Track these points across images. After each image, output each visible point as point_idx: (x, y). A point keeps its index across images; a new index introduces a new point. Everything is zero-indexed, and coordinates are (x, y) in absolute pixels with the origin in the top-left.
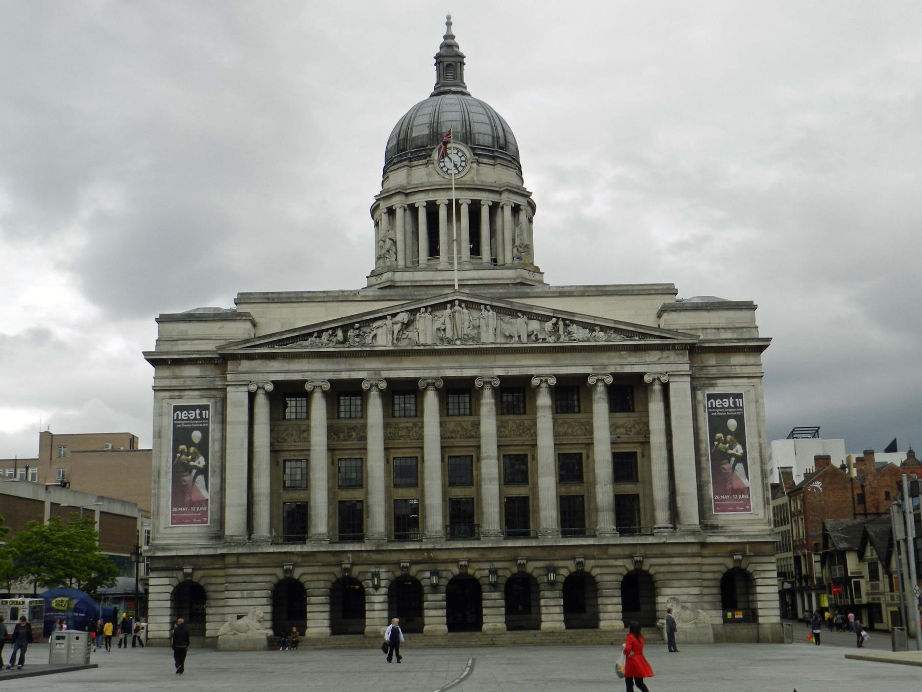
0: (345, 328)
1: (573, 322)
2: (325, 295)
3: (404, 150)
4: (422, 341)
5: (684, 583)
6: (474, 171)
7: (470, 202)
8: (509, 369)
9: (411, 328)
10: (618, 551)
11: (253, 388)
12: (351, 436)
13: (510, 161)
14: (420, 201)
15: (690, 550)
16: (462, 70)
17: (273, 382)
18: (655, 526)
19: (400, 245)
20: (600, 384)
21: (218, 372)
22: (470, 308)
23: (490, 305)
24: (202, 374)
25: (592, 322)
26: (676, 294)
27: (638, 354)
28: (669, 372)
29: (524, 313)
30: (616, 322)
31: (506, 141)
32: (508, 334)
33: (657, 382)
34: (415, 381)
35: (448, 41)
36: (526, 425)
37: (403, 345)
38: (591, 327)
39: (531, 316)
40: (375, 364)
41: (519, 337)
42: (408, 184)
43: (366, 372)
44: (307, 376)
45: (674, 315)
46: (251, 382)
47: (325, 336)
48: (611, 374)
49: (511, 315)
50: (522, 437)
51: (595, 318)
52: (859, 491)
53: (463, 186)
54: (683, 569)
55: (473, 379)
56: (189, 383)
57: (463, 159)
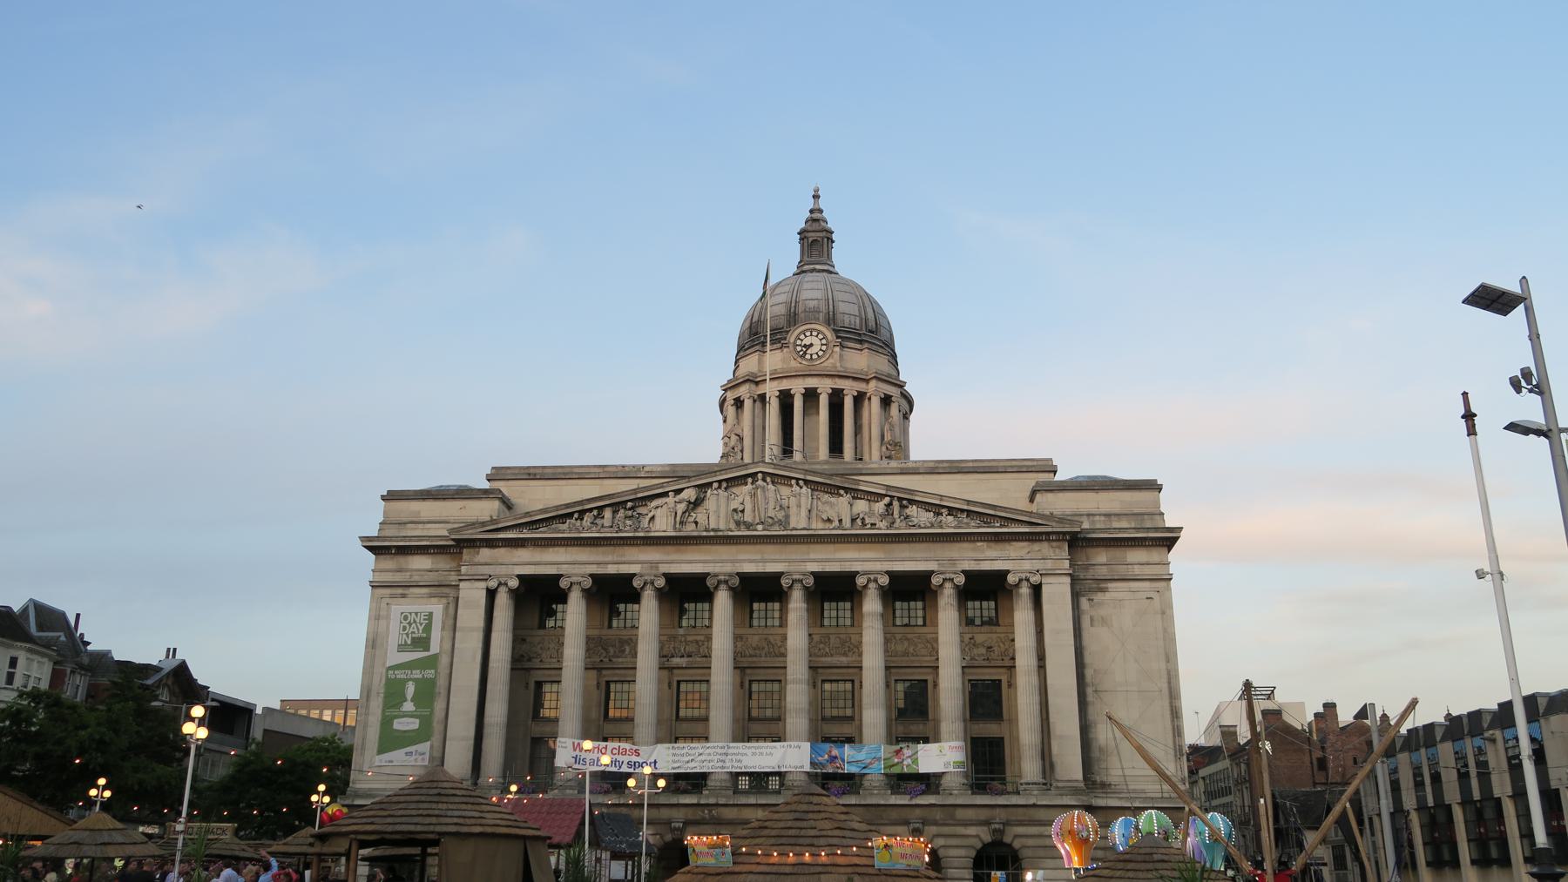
0: (616, 506)
1: (912, 502)
2: (600, 470)
3: (756, 333)
4: (711, 527)
6: (836, 356)
7: (830, 391)
8: (827, 564)
9: (700, 509)
10: (970, 814)
11: (493, 584)
12: (624, 651)
13: (881, 347)
14: (771, 389)
16: (830, 249)
17: (519, 576)
18: (1022, 781)
19: (747, 442)
20: (948, 585)
21: (454, 565)
22: (777, 483)
23: (803, 480)
24: (434, 566)
25: (937, 502)
26: (1055, 472)
27: (1000, 546)
28: (1042, 570)
29: (847, 490)
30: (969, 502)
31: (876, 324)
32: (826, 518)
33: (1025, 584)
34: (702, 577)
35: (816, 215)
36: (852, 641)
37: (690, 529)
39: (856, 494)
41: (840, 521)
42: (760, 371)
43: (640, 565)
44: (563, 570)
45: (1050, 496)
46: (490, 576)
47: (588, 518)
48: (963, 572)
49: (830, 493)
50: (847, 656)
51: (941, 497)
52: (1319, 754)
53: (823, 373)
55: (778, 576)
56: (416, 578)
57: (824, 341)
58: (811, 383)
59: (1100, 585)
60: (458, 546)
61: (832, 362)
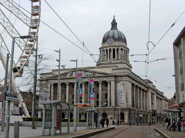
0: (63, 75)
5: (112, 115)
11: (51, 84)
14: (105, 49)
15: (112, 110)
34: (73, 83)
35: (114, 20)
37: (71, 77)
38: (99, 73)
40: (67, 80)
54: (111, 113)
58: (110, 48)
59: (119, 82)
60: (47, 80)
61: (113, 45)
